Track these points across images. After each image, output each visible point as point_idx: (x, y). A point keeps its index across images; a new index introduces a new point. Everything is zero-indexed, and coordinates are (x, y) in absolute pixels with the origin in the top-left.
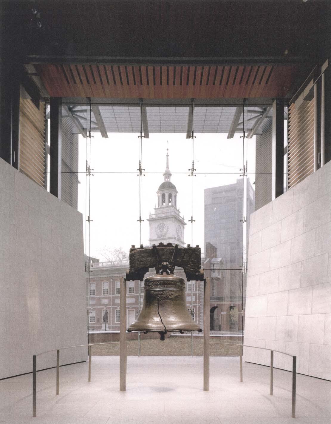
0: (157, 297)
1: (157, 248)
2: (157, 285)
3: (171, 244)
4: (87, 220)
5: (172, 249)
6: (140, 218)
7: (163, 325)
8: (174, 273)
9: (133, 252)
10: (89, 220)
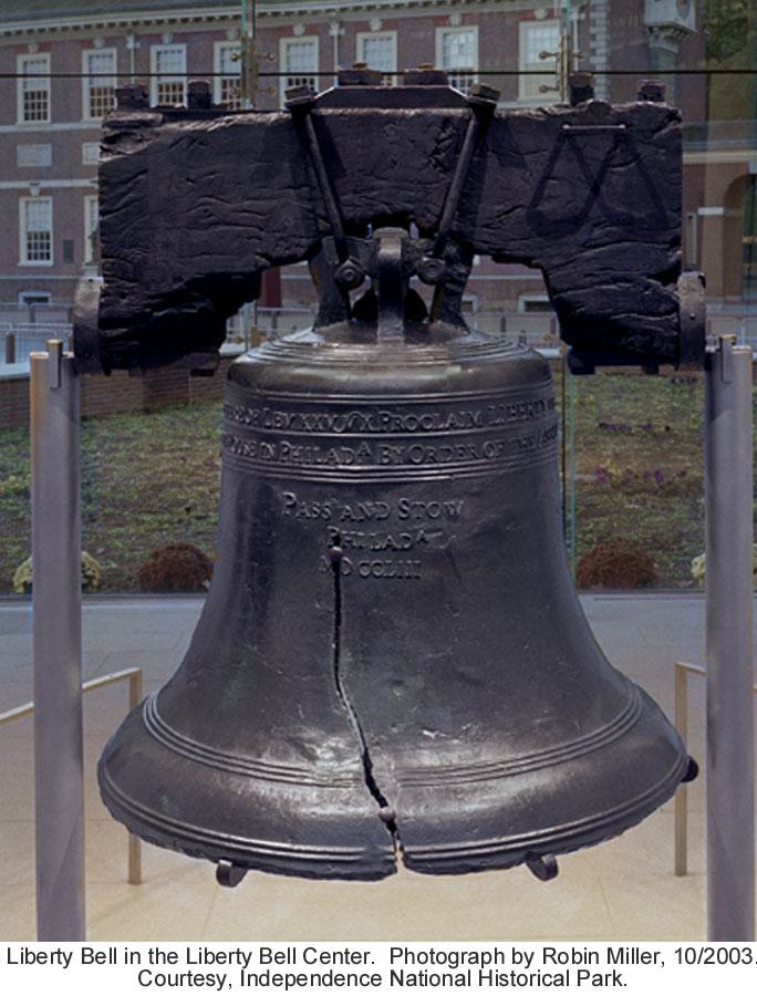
0: (321, 539)
2: (327, 444)
5: (447, 121)
7: (378, 809)
8: (465, 315)
9: (129, 149)
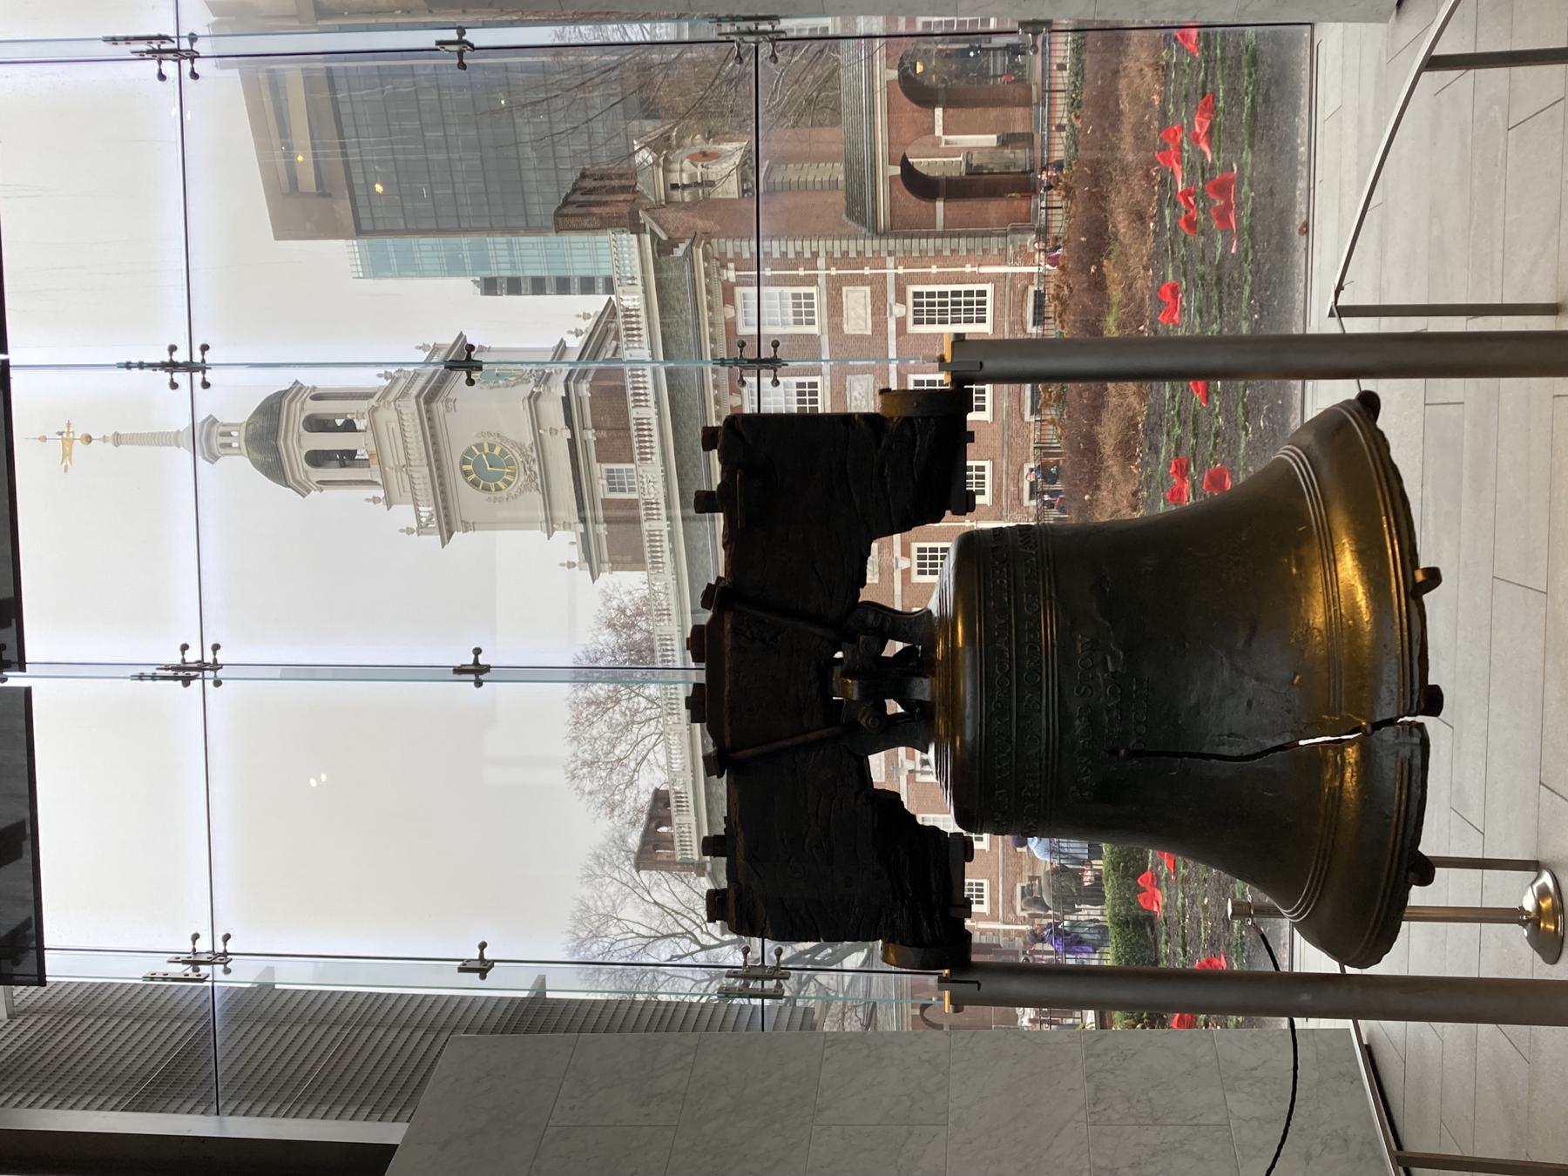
1: (728, 741)
3: (697, 630)
4: (483, 977)
5: (736, 632)
6: (459, 670)
10: (477, 965)
